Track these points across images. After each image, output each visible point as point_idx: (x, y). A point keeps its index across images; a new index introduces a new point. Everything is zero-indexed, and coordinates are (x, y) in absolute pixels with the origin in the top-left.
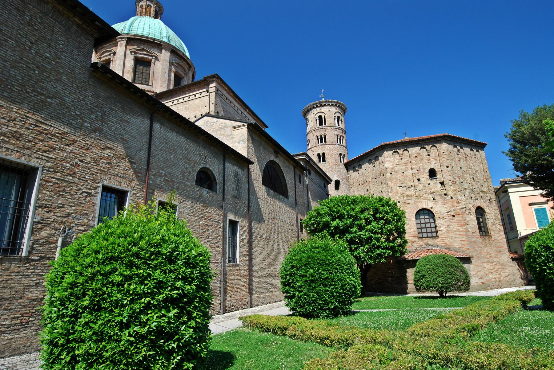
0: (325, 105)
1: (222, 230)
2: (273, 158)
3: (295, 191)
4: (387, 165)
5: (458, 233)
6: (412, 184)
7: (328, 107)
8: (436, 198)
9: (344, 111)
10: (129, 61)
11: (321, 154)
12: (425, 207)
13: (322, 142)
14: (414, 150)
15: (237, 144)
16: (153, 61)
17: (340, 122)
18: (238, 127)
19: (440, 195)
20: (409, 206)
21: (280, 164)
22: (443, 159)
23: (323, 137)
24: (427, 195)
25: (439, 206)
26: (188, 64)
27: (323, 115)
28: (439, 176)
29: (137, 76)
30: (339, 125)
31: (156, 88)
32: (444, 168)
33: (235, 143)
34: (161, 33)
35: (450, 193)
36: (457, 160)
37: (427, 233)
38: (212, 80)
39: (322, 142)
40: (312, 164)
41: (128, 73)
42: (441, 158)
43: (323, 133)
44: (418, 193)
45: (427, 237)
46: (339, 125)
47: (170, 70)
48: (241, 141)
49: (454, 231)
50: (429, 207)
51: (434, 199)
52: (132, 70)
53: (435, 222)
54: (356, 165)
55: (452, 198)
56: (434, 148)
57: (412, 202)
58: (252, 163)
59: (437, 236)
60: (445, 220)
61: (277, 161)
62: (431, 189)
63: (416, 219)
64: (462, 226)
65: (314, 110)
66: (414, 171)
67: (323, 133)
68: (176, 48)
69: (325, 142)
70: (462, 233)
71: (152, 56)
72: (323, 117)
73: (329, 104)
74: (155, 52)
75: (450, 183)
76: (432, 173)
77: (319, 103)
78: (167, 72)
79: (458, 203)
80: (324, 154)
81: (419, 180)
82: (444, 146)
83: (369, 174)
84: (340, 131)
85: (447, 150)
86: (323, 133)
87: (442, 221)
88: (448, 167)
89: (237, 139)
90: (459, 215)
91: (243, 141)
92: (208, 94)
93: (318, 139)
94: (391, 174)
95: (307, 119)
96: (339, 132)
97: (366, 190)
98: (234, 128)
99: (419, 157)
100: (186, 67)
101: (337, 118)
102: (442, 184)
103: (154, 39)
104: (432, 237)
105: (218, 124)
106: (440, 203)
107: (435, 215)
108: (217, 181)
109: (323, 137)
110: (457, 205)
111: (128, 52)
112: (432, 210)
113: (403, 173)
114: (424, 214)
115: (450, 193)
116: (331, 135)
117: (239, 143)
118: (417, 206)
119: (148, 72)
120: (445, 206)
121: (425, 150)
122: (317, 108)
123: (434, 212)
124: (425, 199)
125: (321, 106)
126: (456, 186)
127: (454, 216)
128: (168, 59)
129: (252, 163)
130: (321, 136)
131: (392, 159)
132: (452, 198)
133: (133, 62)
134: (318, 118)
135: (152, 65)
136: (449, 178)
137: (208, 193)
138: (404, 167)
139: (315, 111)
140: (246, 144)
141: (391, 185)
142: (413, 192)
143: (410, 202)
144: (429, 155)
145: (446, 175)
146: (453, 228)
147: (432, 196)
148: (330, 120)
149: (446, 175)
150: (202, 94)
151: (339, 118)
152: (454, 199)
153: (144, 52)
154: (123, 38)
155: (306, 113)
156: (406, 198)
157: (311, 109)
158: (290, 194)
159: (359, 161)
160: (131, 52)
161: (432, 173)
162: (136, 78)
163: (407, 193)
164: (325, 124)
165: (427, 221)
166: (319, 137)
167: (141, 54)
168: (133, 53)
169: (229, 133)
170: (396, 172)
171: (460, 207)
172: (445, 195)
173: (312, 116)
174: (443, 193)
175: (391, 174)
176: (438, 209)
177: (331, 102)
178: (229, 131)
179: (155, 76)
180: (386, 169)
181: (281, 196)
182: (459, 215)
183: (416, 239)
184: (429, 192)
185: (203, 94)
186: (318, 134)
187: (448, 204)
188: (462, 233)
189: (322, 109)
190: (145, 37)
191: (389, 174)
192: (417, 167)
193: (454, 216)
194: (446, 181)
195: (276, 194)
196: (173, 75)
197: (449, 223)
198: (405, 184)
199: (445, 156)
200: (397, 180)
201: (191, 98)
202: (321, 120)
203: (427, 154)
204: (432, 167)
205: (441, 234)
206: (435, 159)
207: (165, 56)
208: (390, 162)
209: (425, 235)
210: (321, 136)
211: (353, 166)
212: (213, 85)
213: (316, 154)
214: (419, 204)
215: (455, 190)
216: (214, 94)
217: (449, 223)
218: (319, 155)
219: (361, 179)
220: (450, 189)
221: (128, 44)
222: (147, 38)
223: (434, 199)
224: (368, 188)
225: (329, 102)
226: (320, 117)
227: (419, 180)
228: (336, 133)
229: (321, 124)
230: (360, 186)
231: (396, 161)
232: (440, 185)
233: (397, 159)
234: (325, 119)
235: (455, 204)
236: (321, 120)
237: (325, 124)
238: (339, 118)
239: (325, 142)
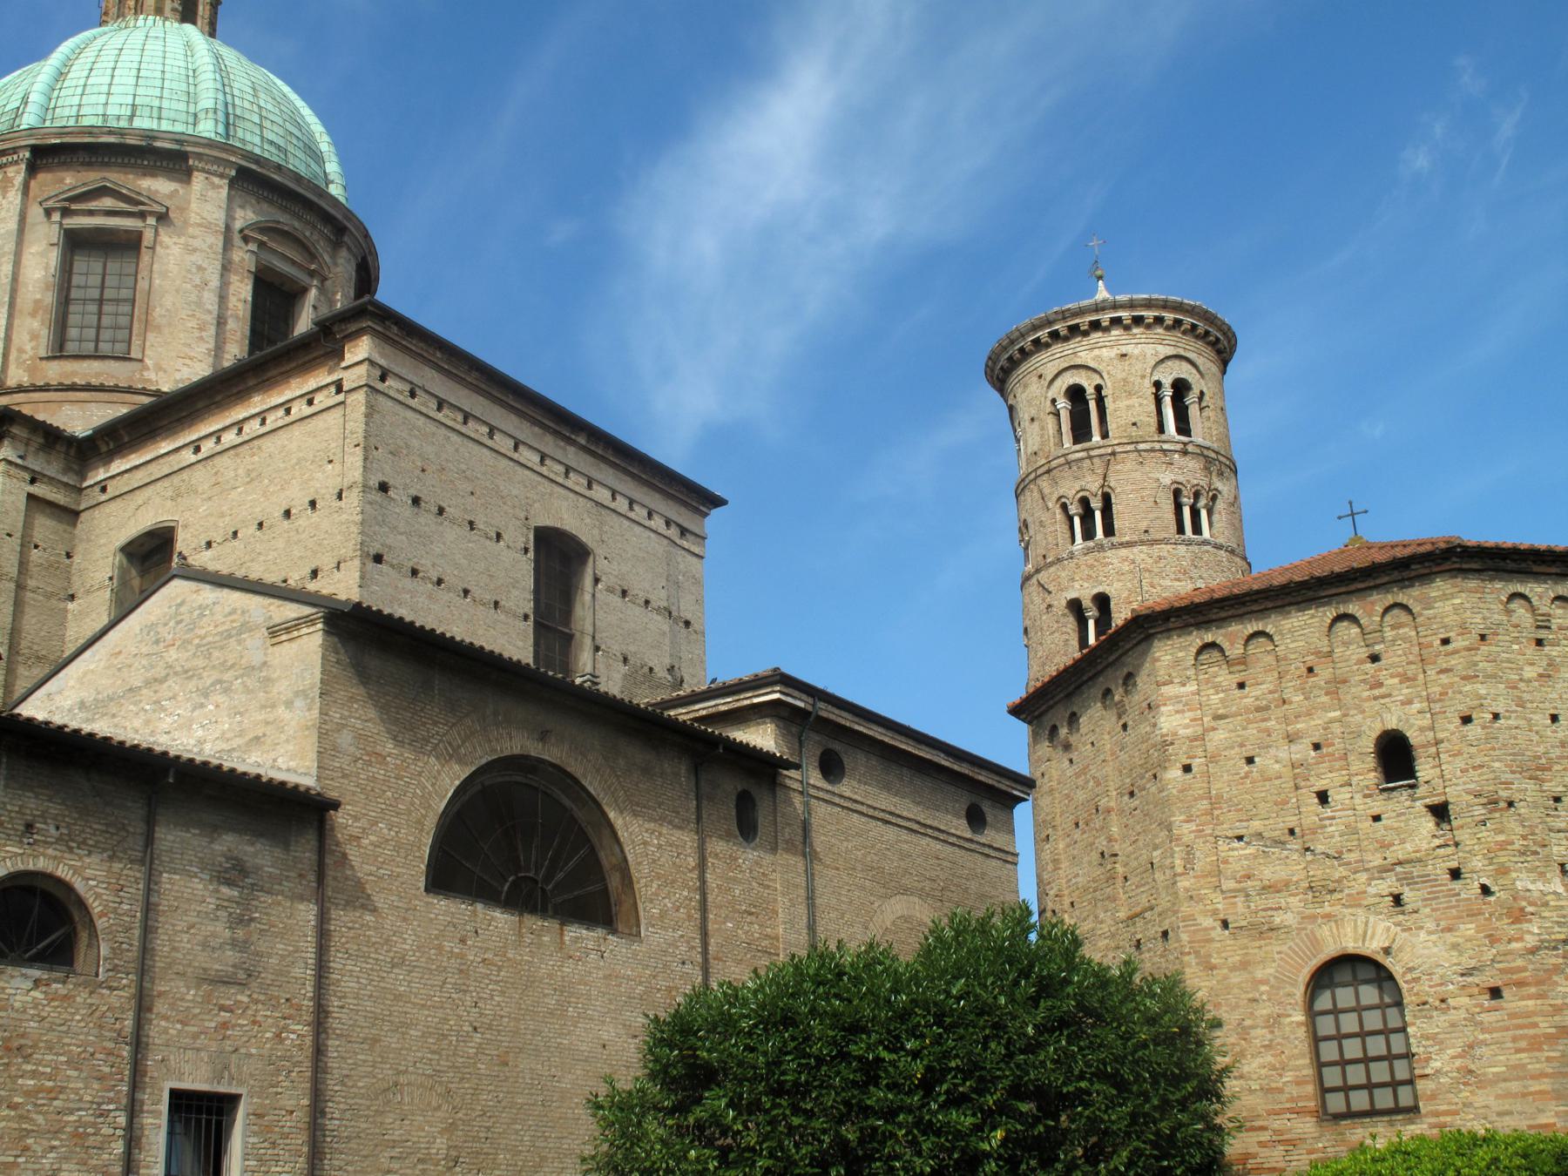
0: (1095, 326)
1: (119, 1147)
2: (517, 743)
3: (703, 890)
4: (1170, 721)
5: (1514, 1086)
6: (1292, 821)
7: (1116, 332)
8: (1408, 895)
9: (1214, 344)
10: (42, 254)
11: (1087, 602)
12: (1351, 946)
13: (1089, 534)
14: (1300, 630)
15: (281, 710)
16: (148, 236)
17: (1193, 411)
18: (288, 630)
19: (1426, 878)
20: (1275, 947)
21: (575, 768)
22: (1444, 679)
23: (1096, 504)
24: (1363, 877)
25: (1423, 935)
26: (327, 218)
27: (1088, 383)
28: (1424, 770)
29: (73, 319)
30: (1183, 427)
31: (159, 368)
32: (1449, 726)
33: (273, 706)
34: (191, 97)
35: (1477, 863)
36: (1530, 672)
37: (1370, 1086)
38: (353, 328)
39: (1089, 534)
40: (846, 720)
41: (33, 314)
42: (1431, 673)
43: (1093, 485)
44: (1317, 872)
45: (1373, 1113)
46: (1183, 427)
47: (226, 268)
48: (297, 694)
49: (1500, 1078)
50: (1372, 947)
51: (1397, 900)
52: (49, 298)
53: (1403, 1030)
54: (1059, 716)
55: (1486, 890)
56: (1403, 617)
57: (1289, 919)
58: (335, 805)
59: (1414, 1109)
60: (1453, 1016)
61: (552, 753)
62: (1384, 846)
63: (1312, 1014)
64: (1535, 1045)
65: (1043, 356)
66: (1302, 750)
67: (1093, 485)
68: (258, 160)
69: (1109, 530)
70: (1535, 1086)
71: (142, 215)
72: (1090, 391)
73: (1116, 322)
74: (159, 187)
75: (1480, 811)
76: (1395, 757)
77: (1064, 315)
78: (215, 282)
79: (1519, 916)
80: (1102, 601)
81: (1323, 797)
82: (1451, 602)
83: (1109, 769)
84: (1193, 464)
85: (1464, 629)
86: (1092, 485)
87: (1440, 1021)
88: (1466, 720)
89: (282, 688)
90: (1520, 984)
91: (303, 693)
92: (341, 397)
93: (1070, 519)
94: (1187, 769)
95: (1011, 408)
96: (1189, 472)
97: (1095, 856)
98: (274, 631)
99: (1324, 673)
100: (316, 237)
101: (1168, 393)
102: (1440, 812)
103: (150, 135)
104: (1397, 1110)
105: (219, 618)
106: (1430, 925)
107: (1404, 987)
108: (101, 924)
109: (1096, 504)
110: (1512, 931)
111: (36, 212)
112: (1387, 962)
113: (1250, 760)
114: (1356, 982)
115: (1479, 869)
116: (1141, 491)
117: (289, 704)
118: (1315, 942)
119: (125, 294)
120: (1450, 938)
121: (1355, 630)
122: (1057, 349)
123: (1397, 970)
124: (1355, 902)
125: (1074, 330)
126: (1513, 825)
127: (1495, 993)
128: (218, 216)
129: (335, 805)
130: (1085, 502)
131: (1192, 687)
132: (1486, 890)
133: (54, 256)
134: (1063, 404)
135: (145, 257)
136: (1474, 781)
137: (37, 983)
138: (1252, 731)
139: (1050, 361)
140: (316, 713)
141: (1186, 830)
142: (1287, 866)
143: (1277, 920)
144: (1375, 658)
145: (1460, 763)
146: (1494, 1062)
147: (1387, 885)
148: (1129, 410)
149: (1460, 763)
150: (318, 398)
151: (1181, 388)
152: (1500, 895)
153: (108, 203)
154: (15, 150)
155: (1002, 371)
156: (1258, 902)
157: (1025, 354)
158: (648, 910)
159: (1069, 696)
160: (48, 212)
161: (1395, 757)
162: (73, 333)
163: (1269, 873)
164: (1105, 435)
165: (1373, 1020)
166: (1074, 509)
167: (91, 213)
168: (56, 217)
169: (256, 658)
170: (1212, 759)
171: (1531, 941)
172: (1455, 874)
173: (1041, 387)
174: (1440, 870)
175: (1187, 769)
176: (1423, 951)
177: (1131, 305)
178: (254, 647)
179: (157, 312)
180: (1166, 744)
181: (574, 932)
182: (1520, 984)
183: (1306, 1126)
184: (1377, 861)
185: (321, 400)
186: (1070, 488)
187: (1468, 929)
188: (1535, 1086)
189: (1083, 350)
190: (111, 132)
191: (1175, 773)
192: (1311, 727)
193: (1495, 993)
194: (1456, 795)
195: (533, 922)
196: (242, 291)
197: (1471, 1034)
198: (1256, 825)
199: (1454, 661)
200: (1215, 802)
201: (273, 420)
202: (1082, 410)
203: (1364, 653)
204: (1392, 723)
205: (1433, 1097)
206: (1406, 679)
207: (205, 202)
208: (1185, 705)
209: (1360, 1100)
210: (1085, 502)
211: (1048, 720)
212: (361, 349)
213: (1060, 602)
214: (1325, 932)
215: (1502, 846)
216: (360, 396)
217: (1471, 1034)
218: (1075, 606)
219: (1081, 796)
220: (1475, 843)
221: (32, 169)
222: (121, 132)
223: (1397, 900)
224: (1102, 843)
225: (1116, 306)
226: (1076, 394)
227: (1323, 797)
228: (1167, 478)
229: (1081, 431)
230: (1077, 835)
231: (1215, 698)
232: (1429, 823)
233: (1217, 688)
234: (1100, 401)
235: (1505, 927)
236: (1082, 410)
237: (1105, 435)
238: (1181, 388)
239: (1109, 530)
